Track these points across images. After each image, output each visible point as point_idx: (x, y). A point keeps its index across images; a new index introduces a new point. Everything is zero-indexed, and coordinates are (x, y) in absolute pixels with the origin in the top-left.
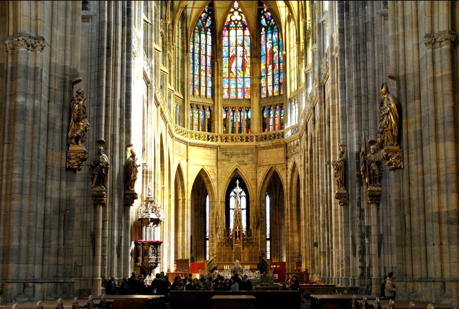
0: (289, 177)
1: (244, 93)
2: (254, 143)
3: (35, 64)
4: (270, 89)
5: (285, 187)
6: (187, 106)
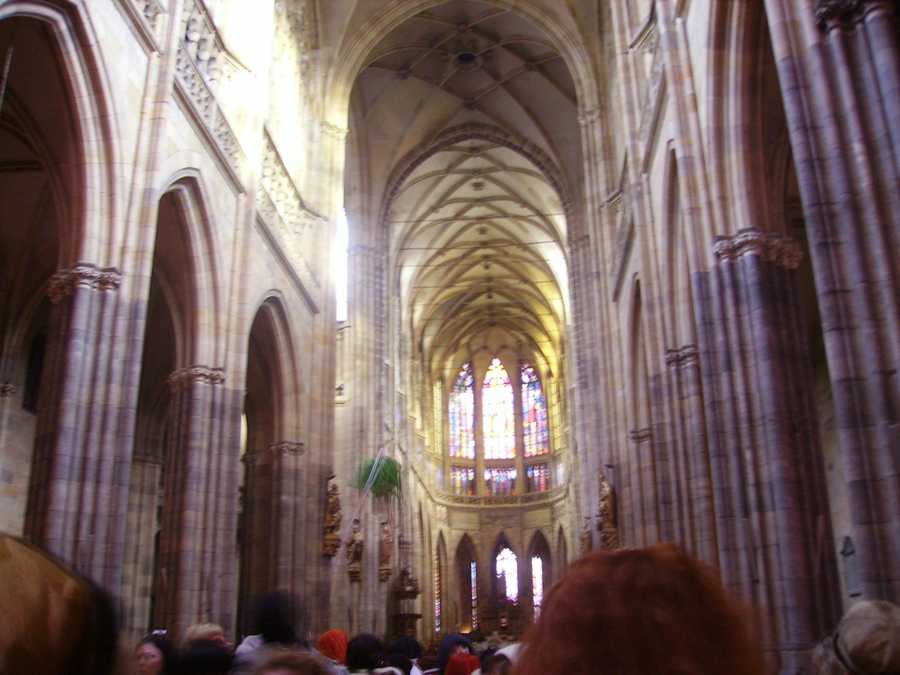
0: (556, 540)
1: (507, 452)
2: (519, 505)
3: (296, 466)
4: (534, 447)
5: (552, 550)
6: (448, 468)
